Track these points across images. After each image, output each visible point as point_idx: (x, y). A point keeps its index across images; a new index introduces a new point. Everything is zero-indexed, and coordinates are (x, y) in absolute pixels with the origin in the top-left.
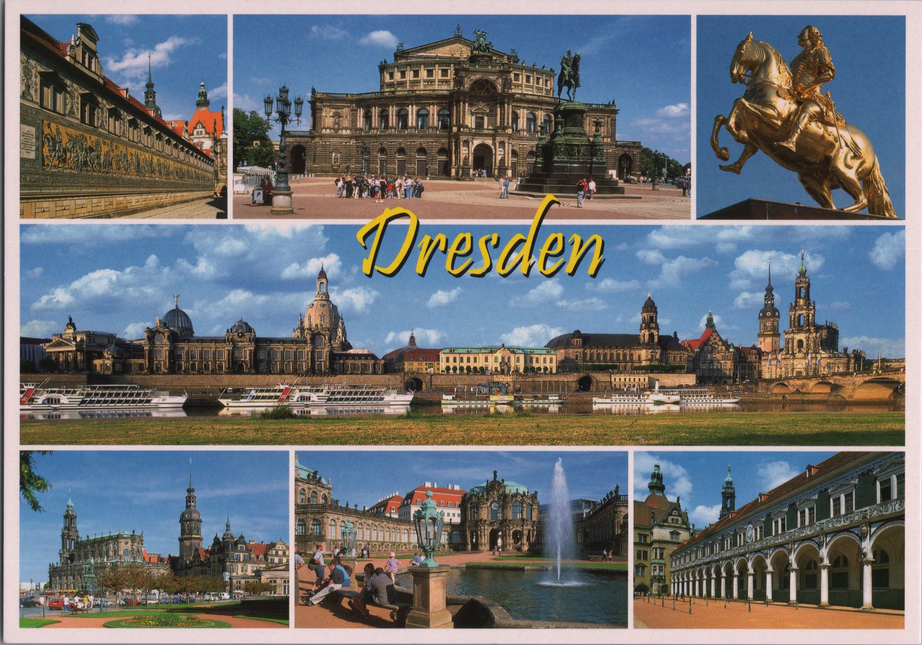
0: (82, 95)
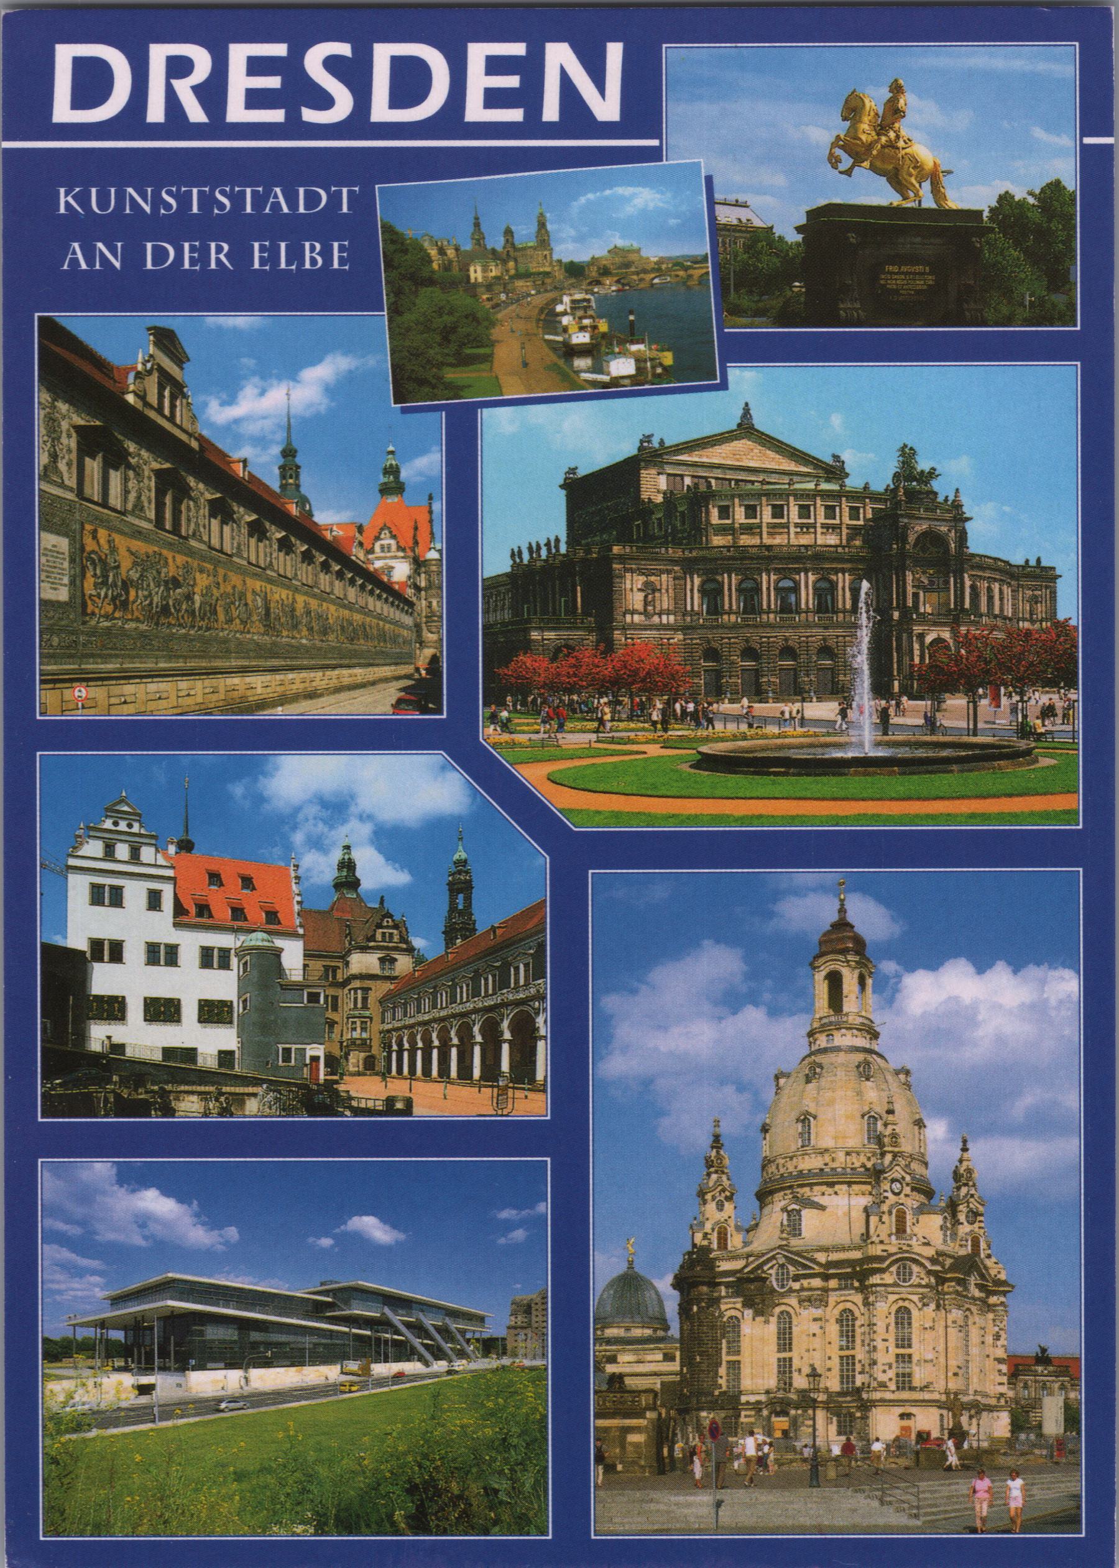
0: (158, 473)
